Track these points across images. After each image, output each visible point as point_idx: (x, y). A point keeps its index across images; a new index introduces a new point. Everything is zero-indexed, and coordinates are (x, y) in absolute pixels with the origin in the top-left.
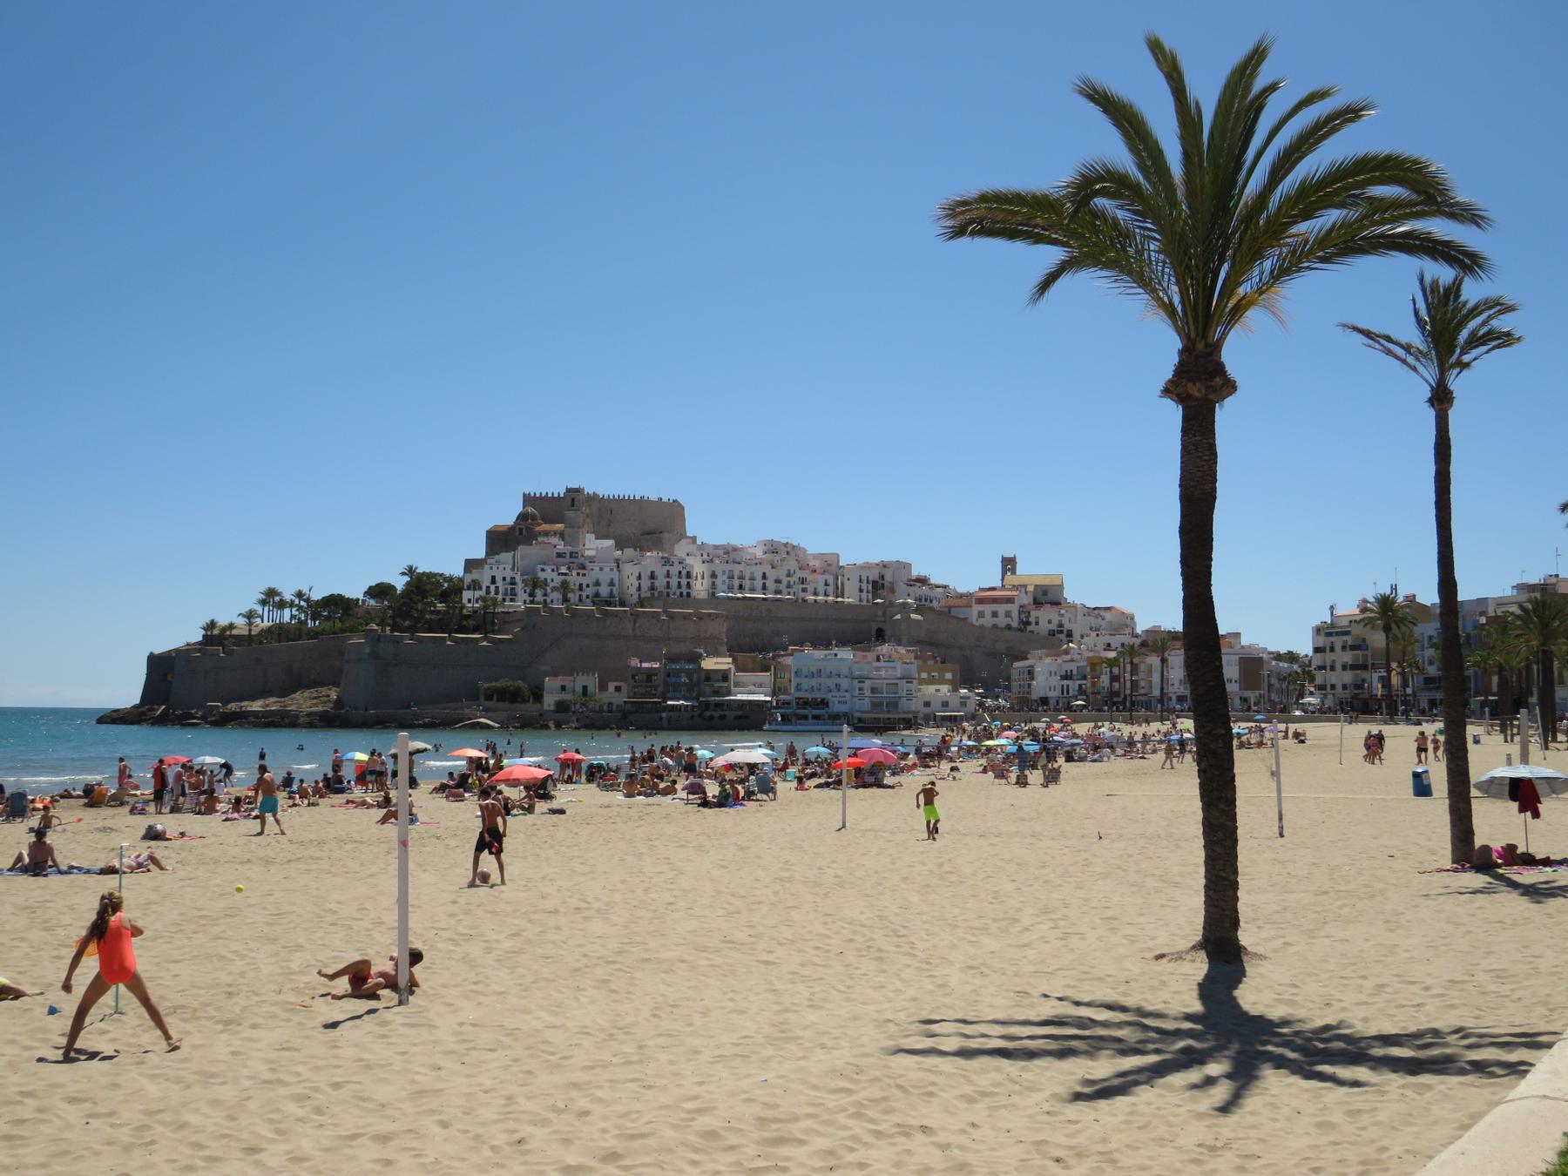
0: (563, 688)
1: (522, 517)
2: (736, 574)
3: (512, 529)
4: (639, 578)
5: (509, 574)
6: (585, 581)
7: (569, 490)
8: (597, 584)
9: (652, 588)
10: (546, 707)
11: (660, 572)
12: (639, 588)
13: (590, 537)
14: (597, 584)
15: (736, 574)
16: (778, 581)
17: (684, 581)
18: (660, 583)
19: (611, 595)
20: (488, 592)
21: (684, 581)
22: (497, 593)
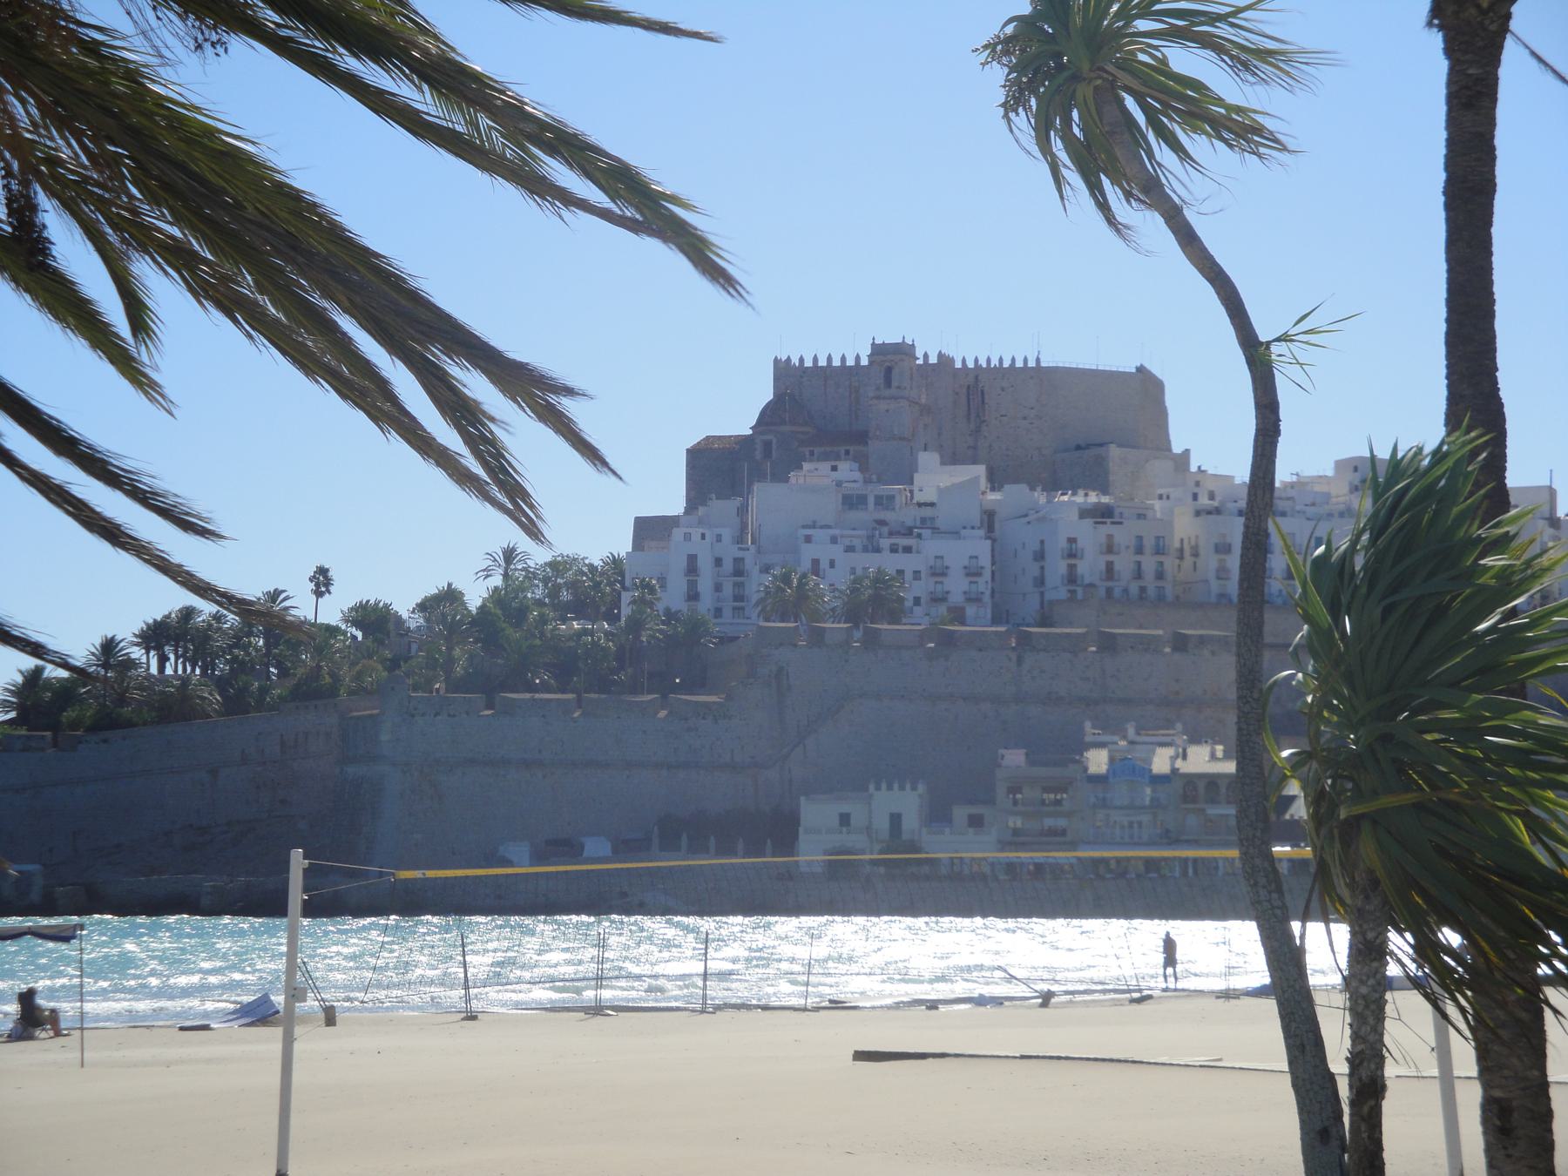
3: (743, 441)
5: (729, 551)
7: (879, 350)
8: (939, 572)
9: (1072, 578)
13: (928, 460)
14: (939, 572)
17: (1149, 563)
18: (1090, 567)
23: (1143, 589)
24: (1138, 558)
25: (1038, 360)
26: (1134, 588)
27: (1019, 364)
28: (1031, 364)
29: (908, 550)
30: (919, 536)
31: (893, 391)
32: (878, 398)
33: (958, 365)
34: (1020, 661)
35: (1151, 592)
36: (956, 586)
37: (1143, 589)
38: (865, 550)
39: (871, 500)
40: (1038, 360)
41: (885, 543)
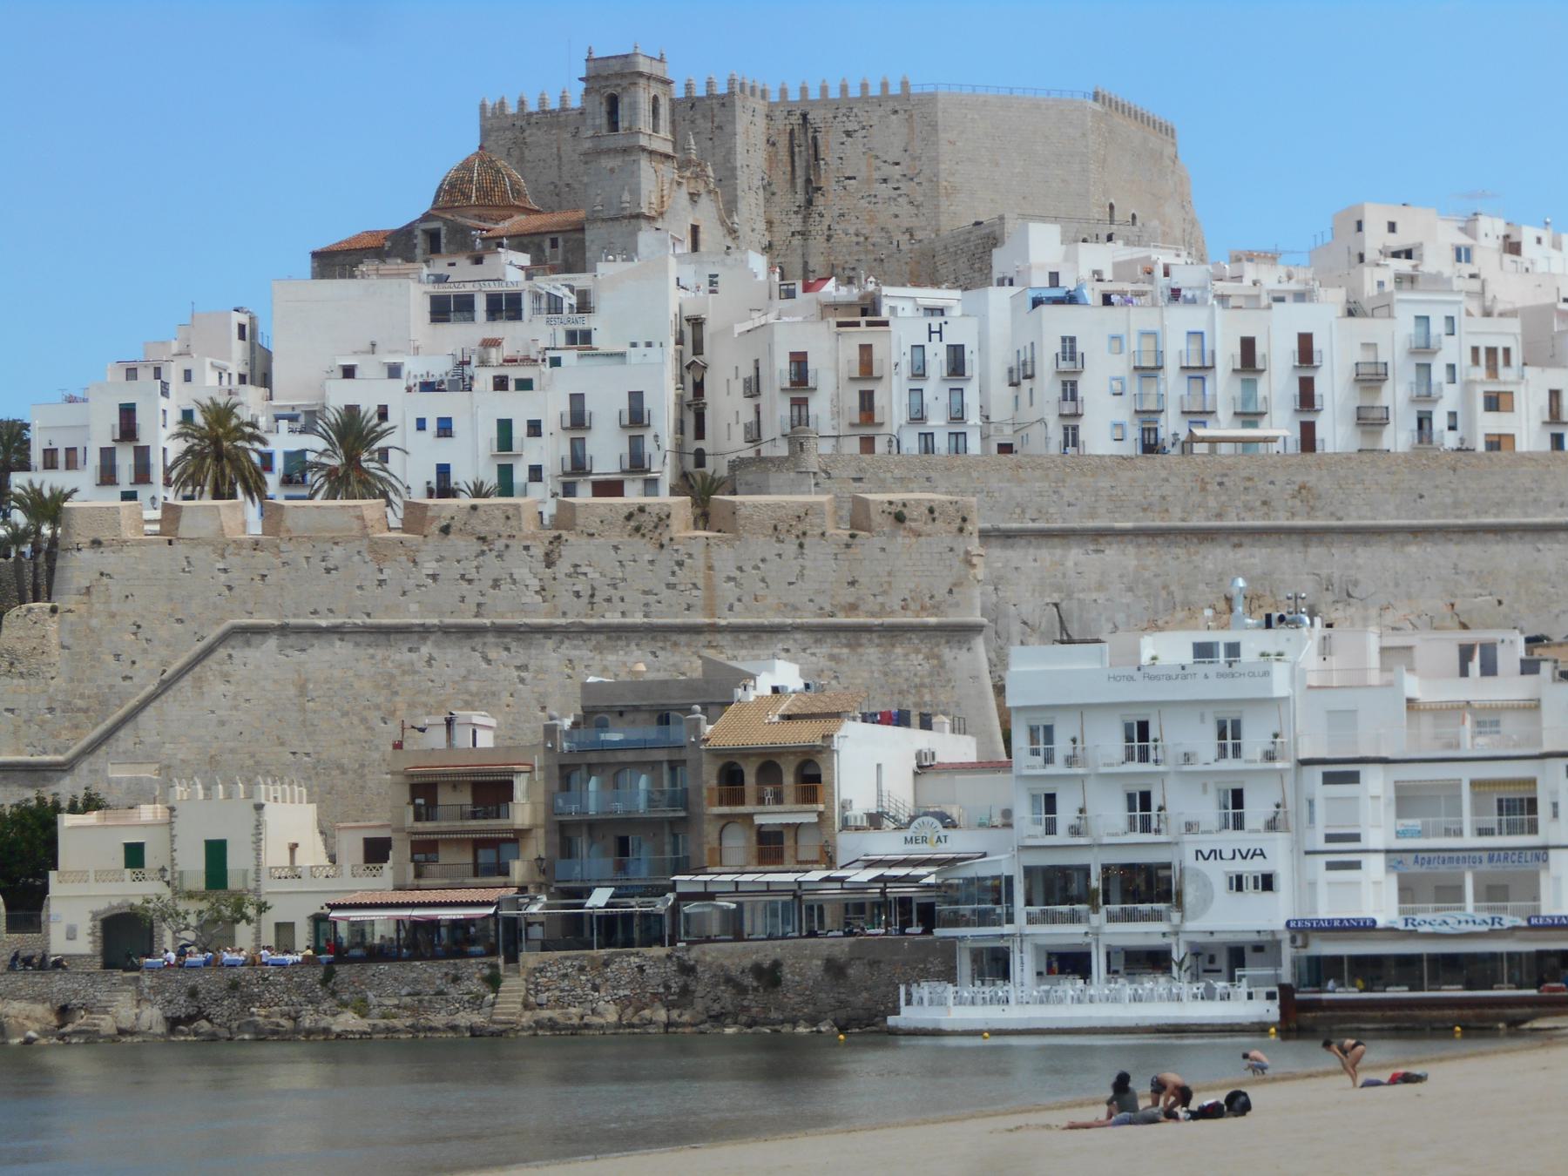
0: (134, 855)
1: (452, 191)
2: (1176, 350)
4: (753, 388)
6: (518, 407)
10: (58, 944)
11: (832, 356)
12: (754, 434)
14: (578, 419)
15: (1176, 350)
19: (637, 463)
20: (108, 476)
22: (142, 474)
25: (905, 84)
27: (875, 91)
28: (895, 89)
29: (525, 385)
30: (556, 362)
31: (619, 140)
33: (774, 97)
35: (941, 443)
37: (927, 438)
38: (454, 387)
39: (481, 305)
40: (905, 84)
41: (484, 378)
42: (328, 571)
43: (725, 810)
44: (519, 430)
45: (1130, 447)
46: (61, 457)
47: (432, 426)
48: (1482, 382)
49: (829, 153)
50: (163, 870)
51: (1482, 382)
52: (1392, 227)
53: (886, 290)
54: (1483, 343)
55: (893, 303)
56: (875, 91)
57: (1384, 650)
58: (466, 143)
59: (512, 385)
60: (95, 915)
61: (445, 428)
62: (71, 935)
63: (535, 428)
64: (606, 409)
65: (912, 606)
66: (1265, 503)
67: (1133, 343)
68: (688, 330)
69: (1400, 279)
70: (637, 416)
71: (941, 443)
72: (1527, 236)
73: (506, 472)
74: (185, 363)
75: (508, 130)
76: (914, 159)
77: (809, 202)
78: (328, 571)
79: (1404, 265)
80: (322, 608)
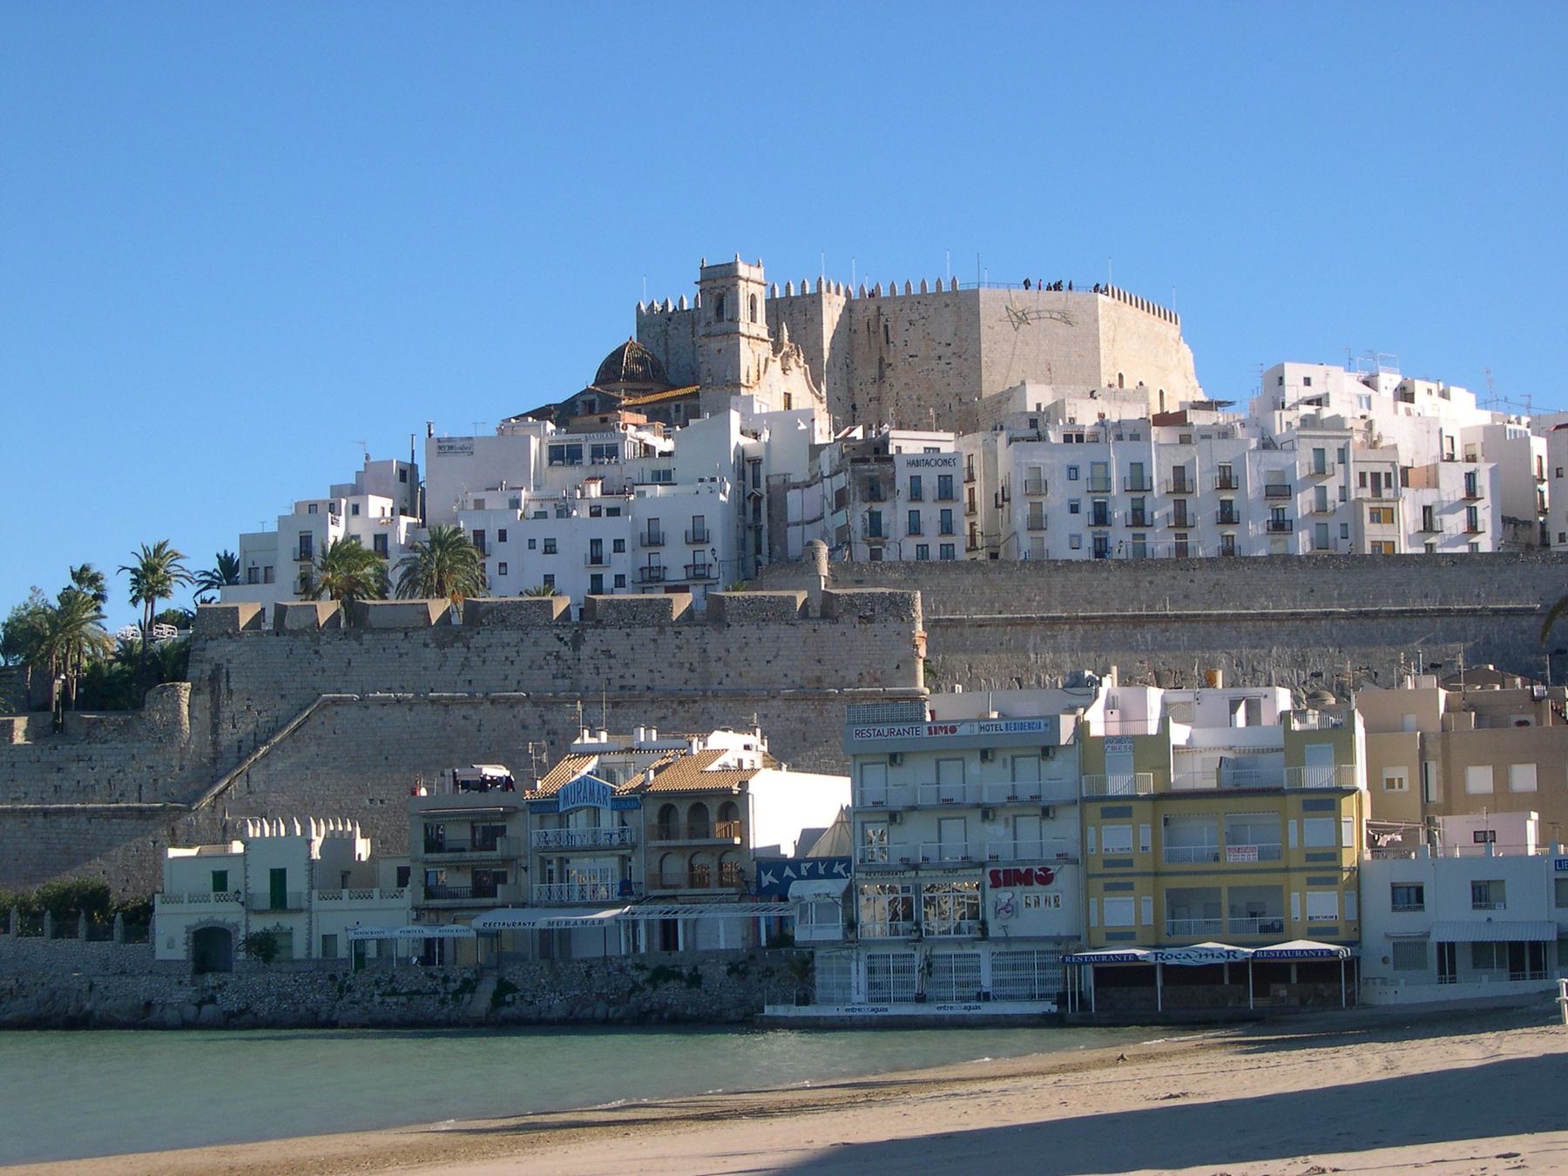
6: (608, 530)
10: (162, 952)
14: (654, 539)
16: (1279, 491)
17: (930, 512)
21: (930, 512)
23: (923, 550)
24: (915, 506)
26: (910, 549)
29: (613, 512)
31: (725, 325)
32: (708, 335)
34: (577, 642)
35: (934, 553)
36: (675, 558)
37: (923, 550)
42: (401, 655)
43: (663, 843)
44: (608, 547)
45: (1084, 554)
46: (261, 573)
47: (540, 545)
48: (1369, 501)
49: (897, 338)
50: (238, 892)
51: (1369, 501)
52: (1307, 382)
53: (893, 434)
54: (1369, 469)
55: (897, 443)
56: (946, 288)
57: (1165, 705)
58: (623, 332)
59: (604, 512)
60: (188, 928)
61: (550, 548)
62: (170, 944)
63: (619, 545)
64: (675, 528)
65: (867, 678)
66: (1186, 597)
67: (1085, 473)
68: (749, 469)
69: (1306, 422)
70: (698, 537)
71: (934, 553)
72: (1420, 388)
73: (597, 581)
74: (354, 500)
75: (655, 324)
76: (961, 340)
77: (881, 377)
78: (401, 655)
79: (1311, 410)
80: (396, 685)
